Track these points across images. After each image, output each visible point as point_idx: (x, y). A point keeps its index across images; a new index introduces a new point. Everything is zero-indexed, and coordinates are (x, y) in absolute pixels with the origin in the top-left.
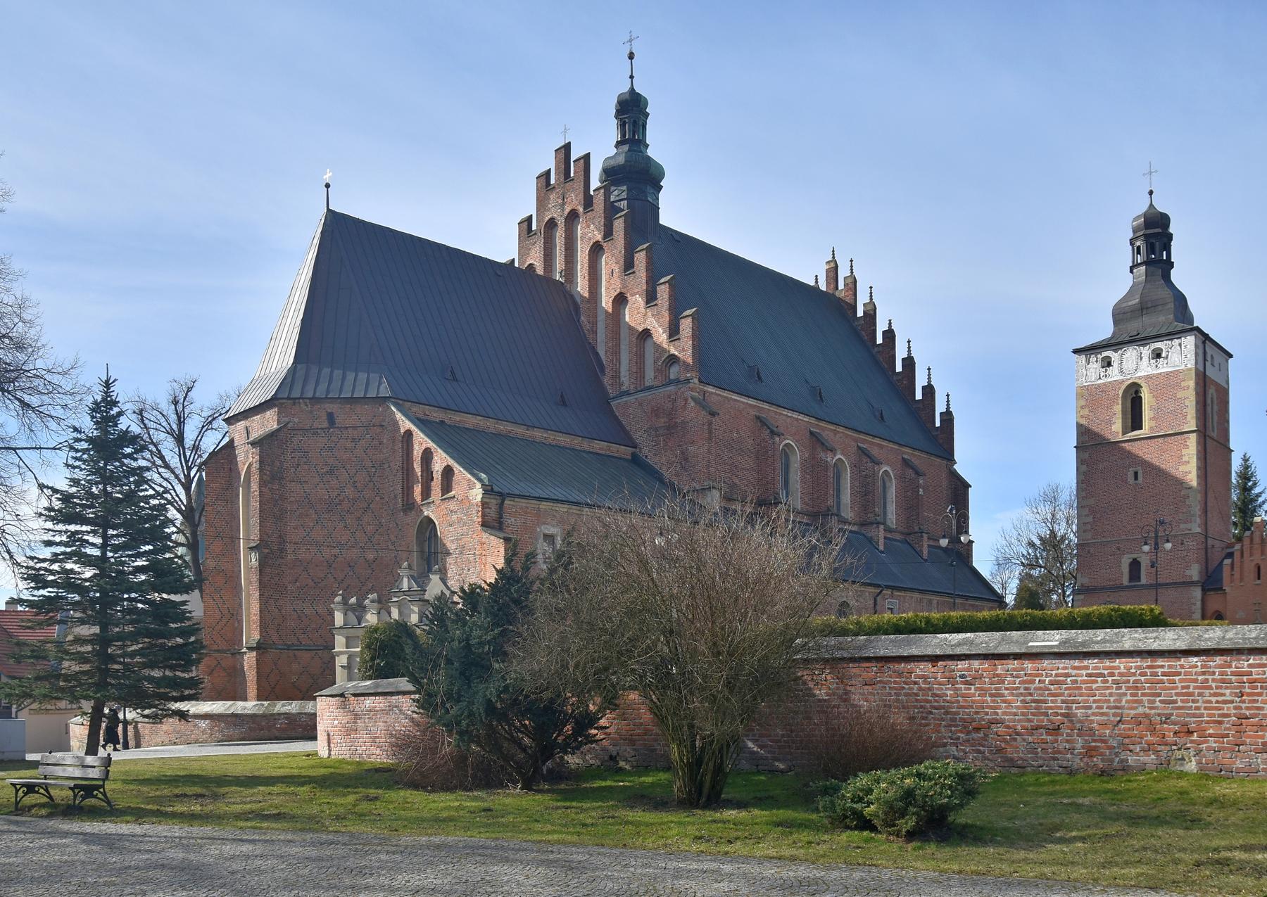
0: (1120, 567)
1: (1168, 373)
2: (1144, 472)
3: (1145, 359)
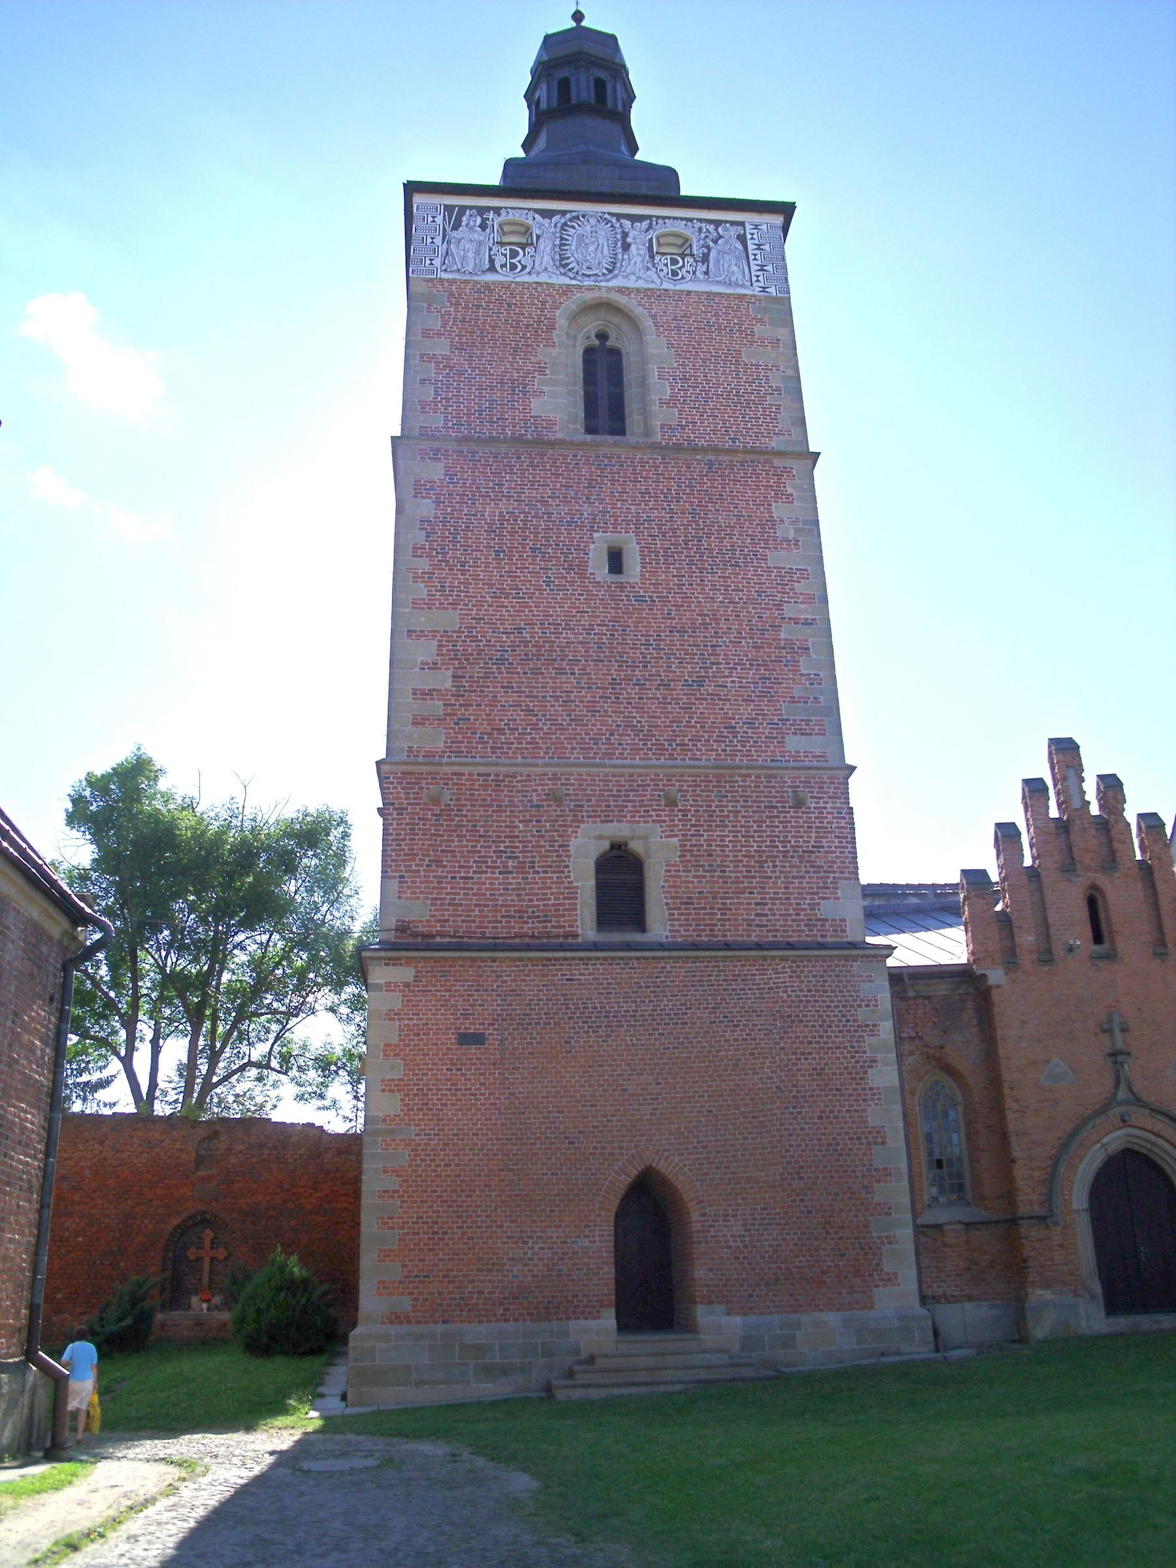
0: (561, 868)
2: (646, 552)
3: (638, 251)
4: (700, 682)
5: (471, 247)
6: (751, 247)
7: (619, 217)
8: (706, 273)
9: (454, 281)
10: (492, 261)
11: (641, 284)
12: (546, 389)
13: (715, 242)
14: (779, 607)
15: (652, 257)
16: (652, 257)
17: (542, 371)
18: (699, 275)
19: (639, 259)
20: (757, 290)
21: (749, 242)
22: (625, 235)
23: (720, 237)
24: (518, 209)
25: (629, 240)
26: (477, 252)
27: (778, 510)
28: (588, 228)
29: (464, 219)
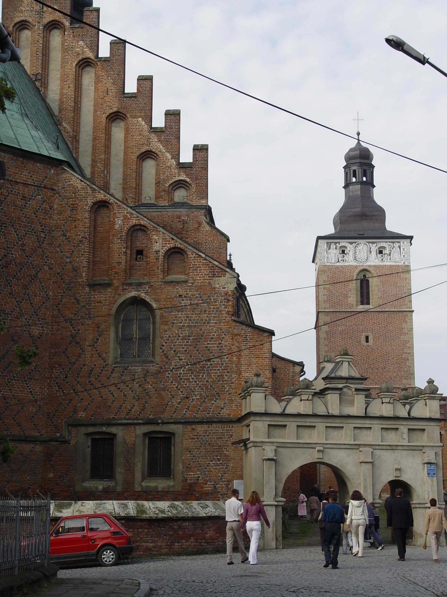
1: (391, 266)
2: (374, 337)
3: (374, 253)
4: (385, 368)
5: (333, 255)
6: (402, 249)
7: (369, 242)
8: (390, 259)
9: (329, 266)
10: (338, 259)
11: (374, 264)
12: (352, 296)
13: (393, 249)
14: (403, 350)
15: (377, 255)
16: (377, 255)
17: (350, 291)
18: (388, 260)
19: (374, 256)
20: (402, 264)
21: (401, 248)
22: (370, 248)
23: (394, 247)
24: (344, 243)
25: (371, 250)
26: (335, 256)
27: (404, 325)
28: (361, 247)
29: (331, 246)
